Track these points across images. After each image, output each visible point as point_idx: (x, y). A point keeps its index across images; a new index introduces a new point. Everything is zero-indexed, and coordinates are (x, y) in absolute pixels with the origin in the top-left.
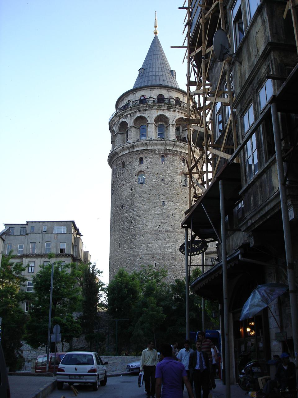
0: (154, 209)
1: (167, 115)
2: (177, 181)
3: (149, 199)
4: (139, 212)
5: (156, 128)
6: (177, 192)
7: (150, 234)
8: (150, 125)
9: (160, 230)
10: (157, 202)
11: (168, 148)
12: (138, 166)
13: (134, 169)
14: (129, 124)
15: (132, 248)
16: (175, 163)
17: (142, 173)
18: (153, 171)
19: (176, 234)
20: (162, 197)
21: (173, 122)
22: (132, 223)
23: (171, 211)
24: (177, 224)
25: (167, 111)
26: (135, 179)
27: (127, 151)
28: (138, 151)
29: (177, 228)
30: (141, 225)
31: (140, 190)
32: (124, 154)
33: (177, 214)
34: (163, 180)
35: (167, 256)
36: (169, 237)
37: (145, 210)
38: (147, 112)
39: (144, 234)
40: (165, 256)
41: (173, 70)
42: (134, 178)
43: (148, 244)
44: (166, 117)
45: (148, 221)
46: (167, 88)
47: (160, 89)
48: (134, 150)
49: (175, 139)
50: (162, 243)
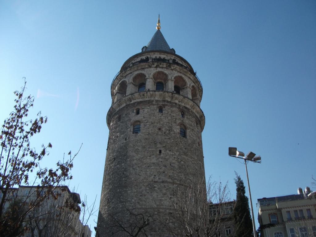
0: (148, 158)
1: (165, 72)
2: (175, 130)
3: (144, 147)
4: (132, 161)
5: (154, 85)
6: (176, 142)
7: (143, 185)
8: (148, 80)
9: (156, 180)
10: (153, 151)
11: (167, 99)
12: (134, 116)
13: (130, 120)
14: (128, 82)
15: (121, 202)
16: (173, 114)
17: (138, 123)
18: (150, 121)
19: (175, 185)
20: (159, 145)
21: (171, 78)
22: (123, 174)
23: (169, 160)
24: (176, 175)
25: (165, 69)
26: (130, 129)
27: (124, 105)
28: (135, 103)
29: (175, 179)
30: (134, 176)
31: (135, 139)
32: (121, 107)
33: (176, 164)
34: (160, 129)
35: (163, 211)
36: (166, 189)
37: (139, 159)
38: (146, 70)
39: (137, 185)
40: (161, 210)
41: (173, 49)
42: (129, 128)
43: (140, 196)
44: (166, 75)
45: (142, 171)
46: (166, 54)
47: (160, 54)
48: (131, 103)
49: (173, 91)
50: (157, 196)
